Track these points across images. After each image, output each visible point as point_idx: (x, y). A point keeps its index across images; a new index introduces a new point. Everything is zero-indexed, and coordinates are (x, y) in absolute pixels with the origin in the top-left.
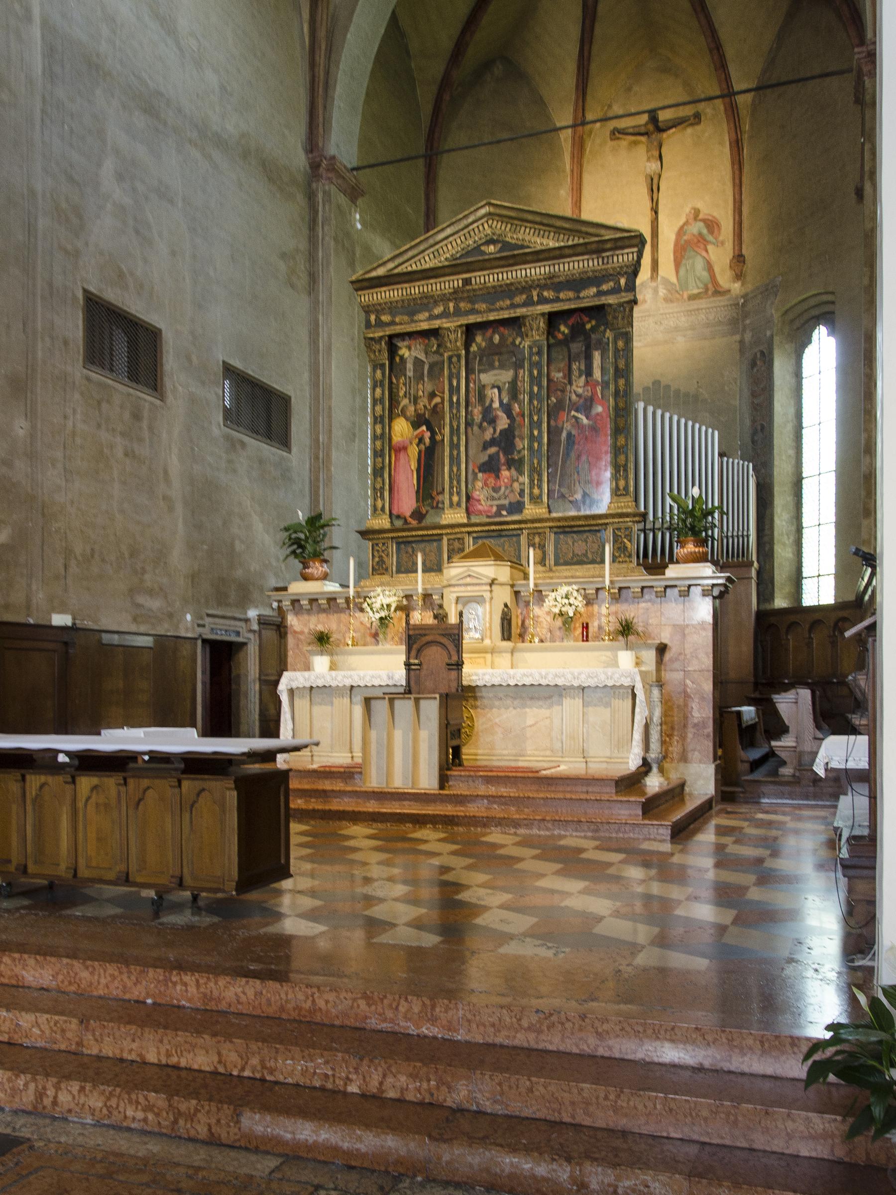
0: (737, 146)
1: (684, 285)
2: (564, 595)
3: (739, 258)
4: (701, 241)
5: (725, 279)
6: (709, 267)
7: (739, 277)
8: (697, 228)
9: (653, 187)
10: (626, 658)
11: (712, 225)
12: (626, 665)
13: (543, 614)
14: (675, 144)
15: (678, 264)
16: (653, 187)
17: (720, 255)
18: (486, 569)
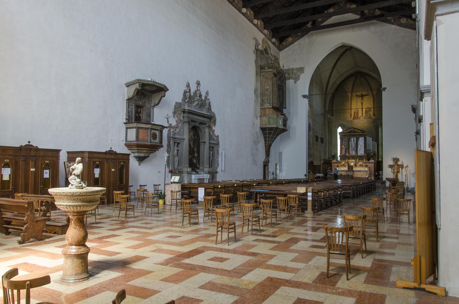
0: (374, 99)
1: (366, 117)
2: (361, 163)
3: (374, 114)
4: (369, 111)
5: (372, 116)
6: (370, 115)
7: (374, 116)
8: (368, 109)
9: (362, 103)
10: (366, 168)
11: (370, 109)
12: (367, 169)
13: (358, 164)
14: (365, 98)
15: (366, 113)
16: (362, 103)
17: (371, 113)
18: (353, 160)
